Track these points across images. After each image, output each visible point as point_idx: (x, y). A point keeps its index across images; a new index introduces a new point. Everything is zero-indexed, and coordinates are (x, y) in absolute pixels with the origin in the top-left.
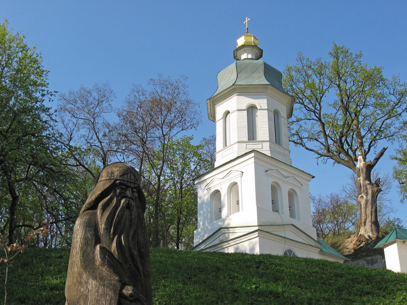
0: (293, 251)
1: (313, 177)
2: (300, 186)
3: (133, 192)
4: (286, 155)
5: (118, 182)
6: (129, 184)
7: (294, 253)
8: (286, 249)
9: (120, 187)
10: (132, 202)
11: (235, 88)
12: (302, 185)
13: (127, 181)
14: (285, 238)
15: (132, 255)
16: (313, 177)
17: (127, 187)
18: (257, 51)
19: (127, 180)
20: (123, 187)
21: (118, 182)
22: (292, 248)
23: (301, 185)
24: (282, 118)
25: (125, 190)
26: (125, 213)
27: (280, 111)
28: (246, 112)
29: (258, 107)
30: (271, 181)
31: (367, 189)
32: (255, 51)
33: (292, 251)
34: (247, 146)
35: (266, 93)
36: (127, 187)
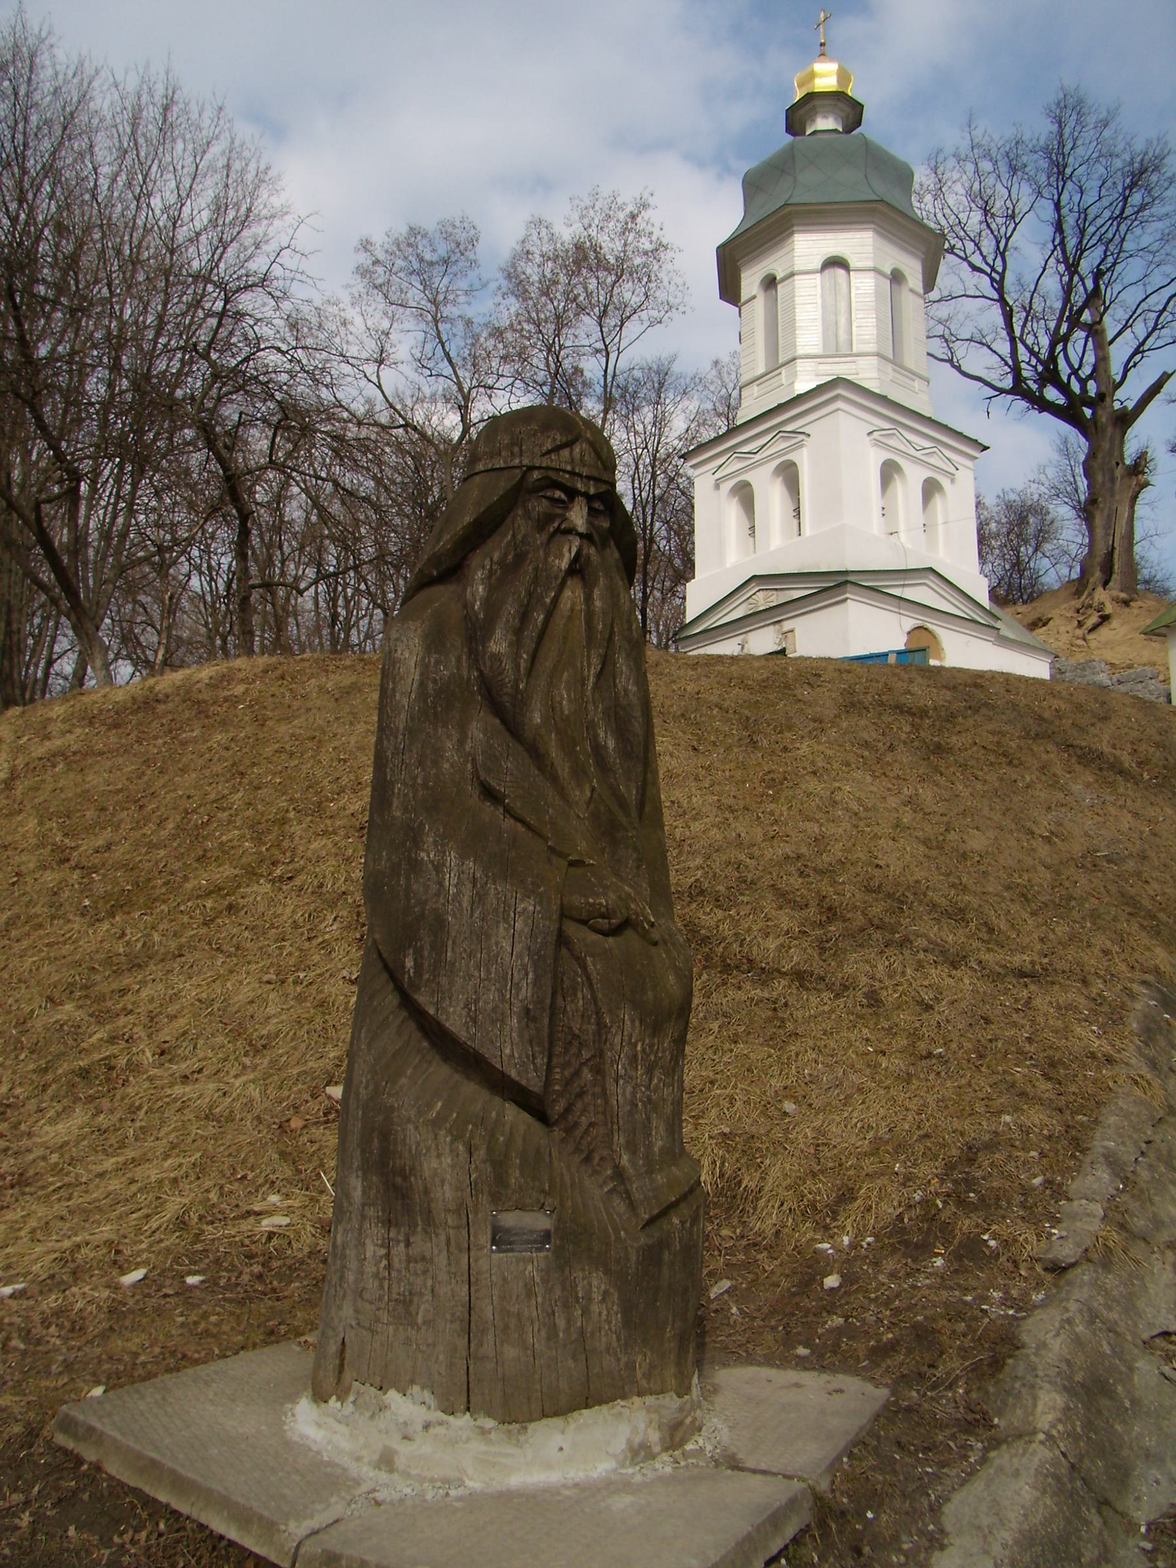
1: (986, 448)
3: (592, 512)
5: (536, 475)
6: (580, 486)
9: (544, 497)
10: (592, 551)
13: (572, 473)
15: (598, 751)
16: (986, 448)
17: (572, 493)
19: (569, 468)
20: (558, 494)
21: (536, 475)
25: (566, 505)
26: (567, 593)
27: (906, 274)
29: (852, 265)
34: (822, 367)
36: (572, 493)
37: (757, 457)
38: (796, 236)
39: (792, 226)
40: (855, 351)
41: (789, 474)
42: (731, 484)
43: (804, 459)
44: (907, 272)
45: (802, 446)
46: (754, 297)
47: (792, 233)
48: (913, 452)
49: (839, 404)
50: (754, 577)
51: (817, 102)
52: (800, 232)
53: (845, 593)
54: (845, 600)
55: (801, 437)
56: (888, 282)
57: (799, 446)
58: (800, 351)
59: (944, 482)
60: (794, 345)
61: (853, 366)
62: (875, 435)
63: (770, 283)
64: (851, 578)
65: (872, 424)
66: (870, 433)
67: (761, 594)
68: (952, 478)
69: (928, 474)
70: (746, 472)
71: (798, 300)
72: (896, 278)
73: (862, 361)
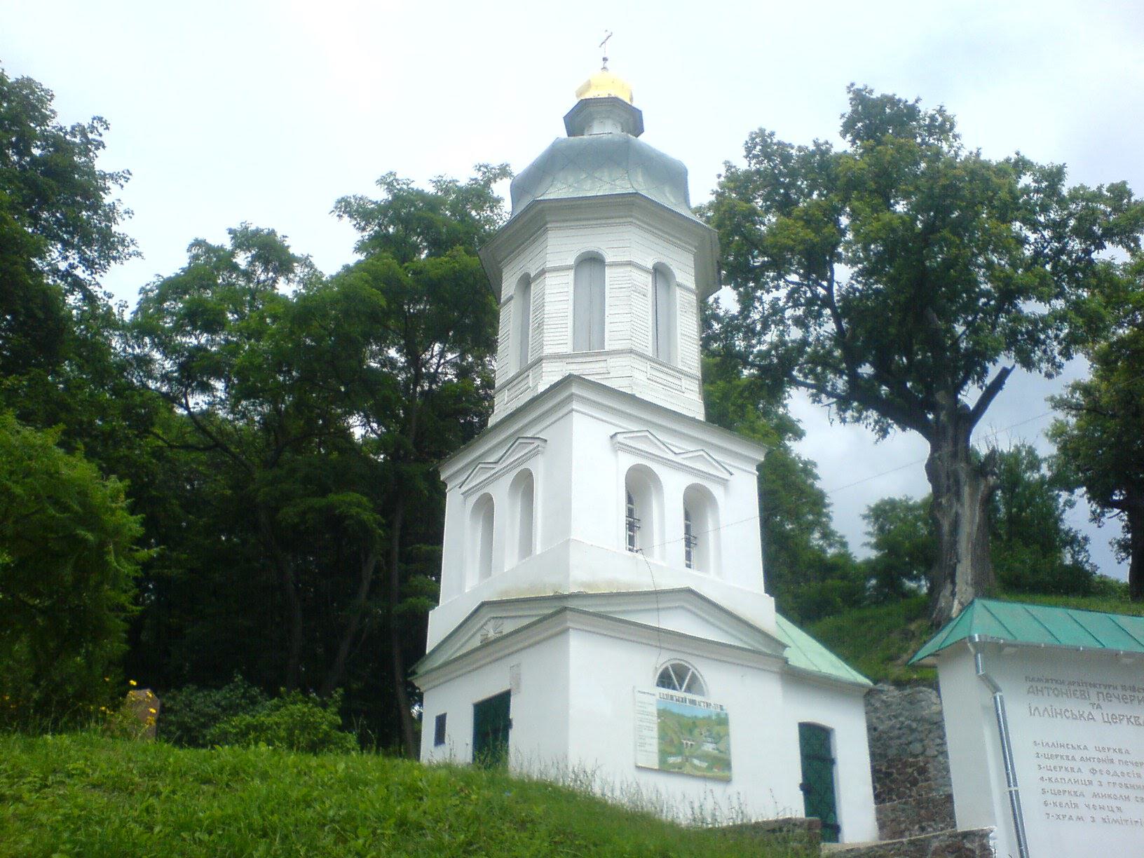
0: (692, 669)
2: (726, 476)
4: (684, 390)
7: (694, 676)
8: (668, 664)
14: (658, 630)
22: (689, 659)
24: (678, 291)
28: (571, 273)
29: (608, 260)
31: (957, 482)
35: (629, 220)
37: (498, 467)
38: (550, 234)
39: (546, 223)
40: (607, 348)
41: (525, 484)
42: (473, 499)
43: (539, 468)
46: (510, 299)
47: (546, 230)
48: (671, 456)
49: (575, 405)
50: (483, 605)
52: (552, 229)
54: (566, 630)
55: (537, 443)
56: (649, 278)
57: (535, 453)
58: (548, 350)
59: (716, 491)
60: (542, 346)
61: (602, 364)
62: (620, 438)
63: (526, 282)
64: (571, 604)
65: (620, 427)
68: (724, 483)
69: (690, 480)
70: (488, 484)
71: (547, 299)
72: (661, 273)
73: (613, 362)
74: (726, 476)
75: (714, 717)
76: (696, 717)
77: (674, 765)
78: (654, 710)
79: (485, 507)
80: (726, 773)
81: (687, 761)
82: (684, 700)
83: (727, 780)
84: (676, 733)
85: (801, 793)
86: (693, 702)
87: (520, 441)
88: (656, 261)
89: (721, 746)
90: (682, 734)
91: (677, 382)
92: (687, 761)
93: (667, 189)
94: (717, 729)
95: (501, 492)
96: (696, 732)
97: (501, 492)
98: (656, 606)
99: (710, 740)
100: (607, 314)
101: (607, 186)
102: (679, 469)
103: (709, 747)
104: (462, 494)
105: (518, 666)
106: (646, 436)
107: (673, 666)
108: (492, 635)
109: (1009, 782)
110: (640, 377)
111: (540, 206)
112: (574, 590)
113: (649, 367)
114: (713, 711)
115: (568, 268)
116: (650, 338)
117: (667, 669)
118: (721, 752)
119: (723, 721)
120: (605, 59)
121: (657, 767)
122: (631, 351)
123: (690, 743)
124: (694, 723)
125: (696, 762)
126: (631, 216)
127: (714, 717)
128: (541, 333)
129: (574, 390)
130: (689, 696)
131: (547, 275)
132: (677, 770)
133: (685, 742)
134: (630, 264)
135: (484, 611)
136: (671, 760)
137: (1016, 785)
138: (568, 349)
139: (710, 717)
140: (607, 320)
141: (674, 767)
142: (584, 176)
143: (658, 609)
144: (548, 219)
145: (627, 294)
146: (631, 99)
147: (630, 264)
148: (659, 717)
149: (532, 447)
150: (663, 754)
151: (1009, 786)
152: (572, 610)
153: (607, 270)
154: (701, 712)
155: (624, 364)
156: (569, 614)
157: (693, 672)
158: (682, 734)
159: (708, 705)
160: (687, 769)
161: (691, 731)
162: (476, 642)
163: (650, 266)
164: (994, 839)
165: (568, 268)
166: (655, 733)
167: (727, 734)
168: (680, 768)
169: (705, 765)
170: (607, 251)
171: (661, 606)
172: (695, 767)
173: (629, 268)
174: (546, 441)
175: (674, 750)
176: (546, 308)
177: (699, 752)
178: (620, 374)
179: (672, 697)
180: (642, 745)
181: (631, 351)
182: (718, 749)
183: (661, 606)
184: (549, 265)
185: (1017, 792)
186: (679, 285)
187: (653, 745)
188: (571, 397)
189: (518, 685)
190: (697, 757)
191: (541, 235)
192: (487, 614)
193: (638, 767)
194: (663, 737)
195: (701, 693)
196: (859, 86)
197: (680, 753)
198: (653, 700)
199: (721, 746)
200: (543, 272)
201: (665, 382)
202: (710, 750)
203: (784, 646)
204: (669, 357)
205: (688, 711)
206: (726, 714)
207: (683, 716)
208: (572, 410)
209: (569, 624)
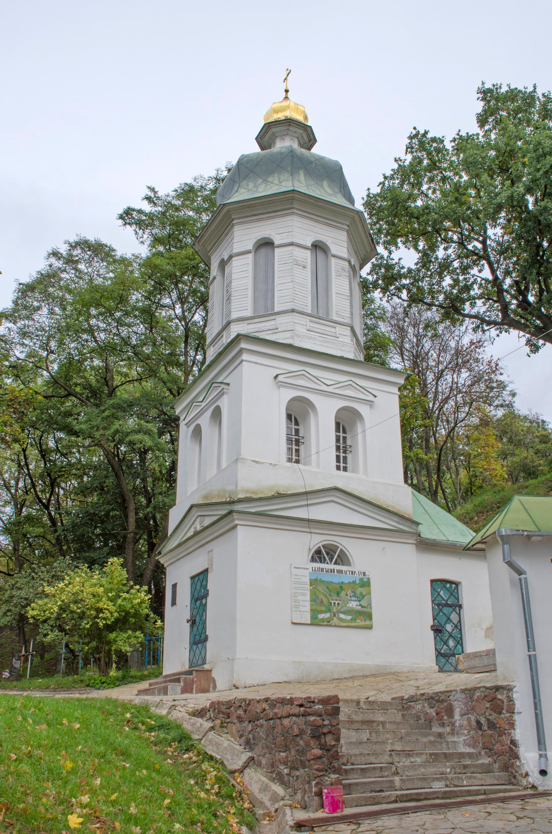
0: (341, 547)
2: (371, 398)
4: (338, 335)
8: (320, 545)
11: (229, 211)
12: (375, 397)
14: (309, 521)
18: (301, 132)
23: (373, 397)
24: (333, 259)
27: (327, 243)
28: (250, 256)
29: (276, 243)
30: (289, 394)
32: (295, 132)
33: (338, 547)
37: (203, 404)
38: (236, 228)
39: (233, 220)
40: (276, 310)
42: (192, 427)
43: (224, 403)
44: (329, 242)
45: (223, 394)
47: (233, 226)
48: (324, 388)
49: (245, 356)
50: (192, 507)
51: (274, 130)
53: (234, 520)
54: (235, 527)
55: (223, 386)
56: (309, 253)
57: (221, 394)
58: (234, 316)
60: (230, 312)
61: (273, 323)
62: (280, 378)
63: (223, 264)
66: (276, 377)
67: (199, 518)
68: (370, 403)
70: (199, 417)
73: (280, 319)
74: (371, 398)
75: (357, 582)
76: (342, 583)
77: (323, 620)
78: (307, 580)
79: (197, 432)
80: (368, 623)
81: (334, 615)
82: (332, 571)
83: (370, 628)
84: (326, 596)
85: (432, 632)
86: (340, 572)
87: (214, 385)
88: (314, 240)
89: (364, 603)
90: (331, 596)
91: (333, 330)
92: (334, 615)
93: (325, 184)
94: (359, 590)
95: (205, 421)
96: (343, 594)
97: (205, 421)
98: (305, 503)
99: (354, 599)
100: (276, 284)
101: (277, 187)
102: (331, 397)
103: (353, 605)
104: (186, 424)
105: (212, 551)
106: (303, 375)
107: (324, 546)
108: (199, 528)
109: (529, 648)
110: (301, 330)
111: (226, 209)
112: (241, 496)
113: (308, 321)
114: (357, 578)
115: (249, 252)
116: (310, 299)
117: (319, 547)
118: (363, 607)
119: (366, 584)
120: (287, 91)
121: (309, 622)
122: (293, 311)
123: (337, 602)
124: (341, 587)
125: (342, 616)
126: (293, 208)
127: (357, 582)
128: (230, 303)
129: (243, 345)
130: (337, 567)
131: (234, 259)
132: (326, 623)
133: (333, 602)
134: (292, 244)
135: (194, 510)
136: (321, 616)
137: (534, 650)
138: (249, 313)
139: (354, 582)
140: (276, 289)
141: (323, 622)
142: (261, 181)
143: (308, 505)
144: (233, 217)
145: (291, 267)
146: (306, 118)
147: (292, 244)
148: (311, 585)
149: (220, 389)
150: (314, 613)
151: (529, 651)
152: (238, 512)
153: (276, 250)
154: (346, 579)
155: (288, 321)
156: (235, 515)
157: (341, 549)
158: (331, 596)
159: (353, 573)
160: (335, 621)
161: (338, 594)
162: (191, 533)
163: (309, 244)
164: (517, 692)
165: (249, 252)
166: (308, 598)
167: (370, 594)
168: (329, 622)
169: (349, 618)
170: (276, 236)
171: (310, 502)
172: (341, 620)
173: (291, 248)
174: (228, 384)
175: (323, 608)
176: (233, 284)
177: (345, 609)
178: (285, 328)
179: (322, 570)
180: (297, 607)
181: (293, 311)
182: (360, 605)
183: (310, 502)
184: (235, 251)
185: (535, 655)
186: (333, 256)
187: (307, 606)
188: (241, 351)
189: (212, 564)
190: (344, 613)
191: (230, 231)
192: (195, 513)
193: (293, 623)
194: (314, 599)
195: (348, 563)
196: (488, 86)
197: (330, 611)
198: (307, 573)
199: (364, 603)
200: (231, 257)
201: (322, 331)
202: (354, 606)
203: (417, 524)
204: (328, 313)
205: (336, 579)
206: (369, 579)
207: (332, 582)
208: (242, 361)
209: (237, 522)
